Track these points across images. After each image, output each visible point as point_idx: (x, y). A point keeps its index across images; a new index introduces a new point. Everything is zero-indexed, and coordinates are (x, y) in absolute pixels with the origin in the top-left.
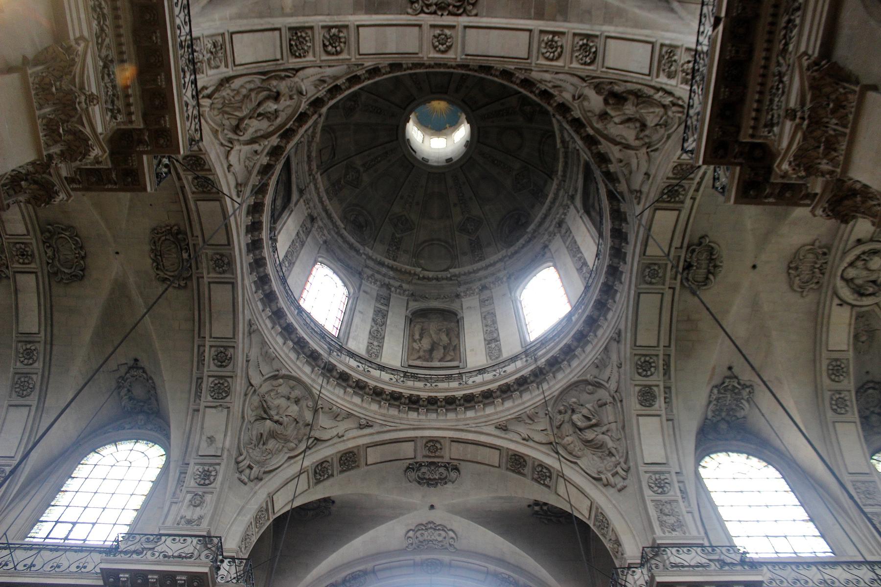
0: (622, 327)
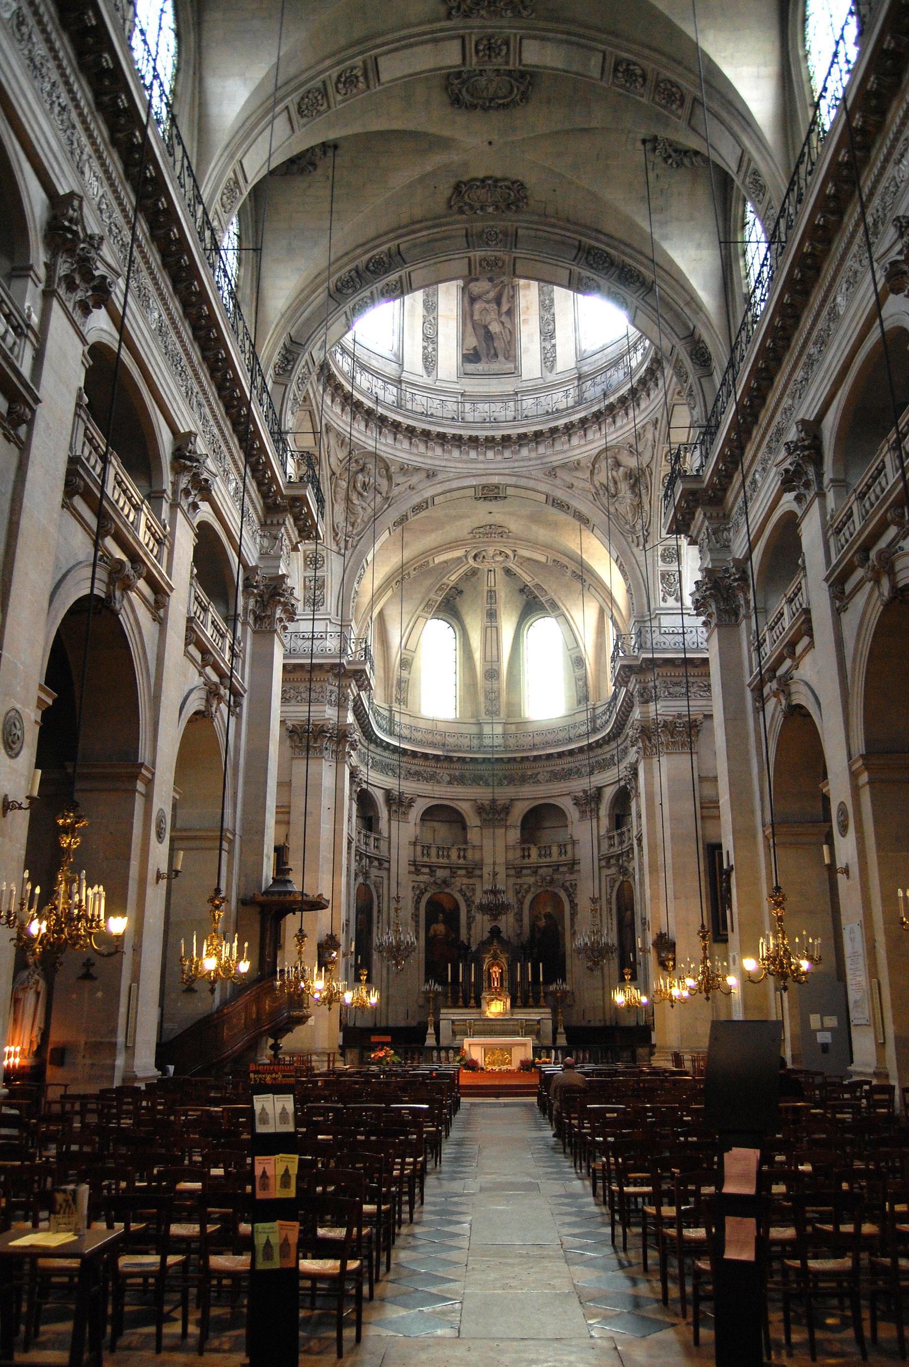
0: (441, 477)
